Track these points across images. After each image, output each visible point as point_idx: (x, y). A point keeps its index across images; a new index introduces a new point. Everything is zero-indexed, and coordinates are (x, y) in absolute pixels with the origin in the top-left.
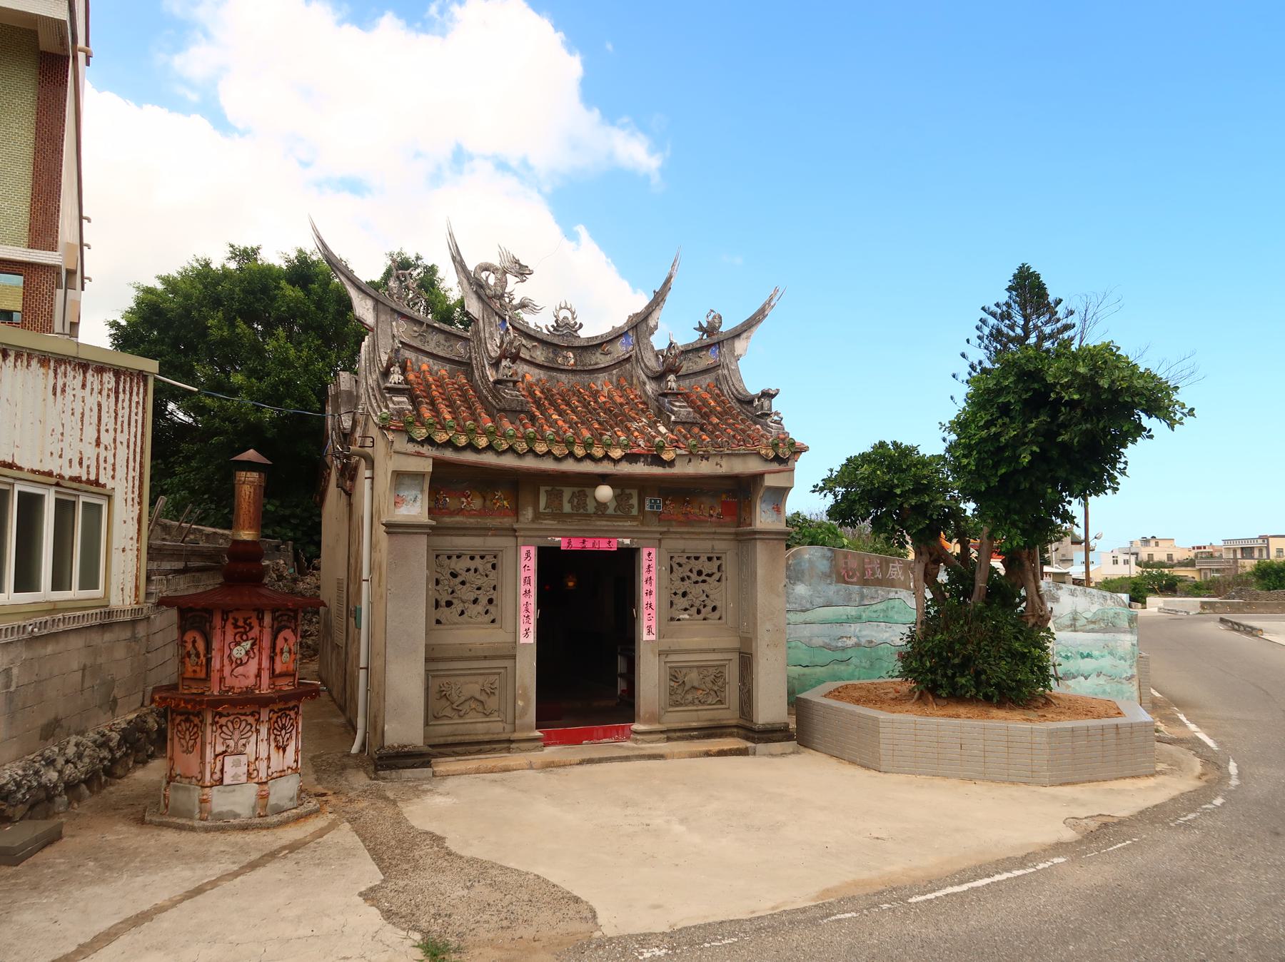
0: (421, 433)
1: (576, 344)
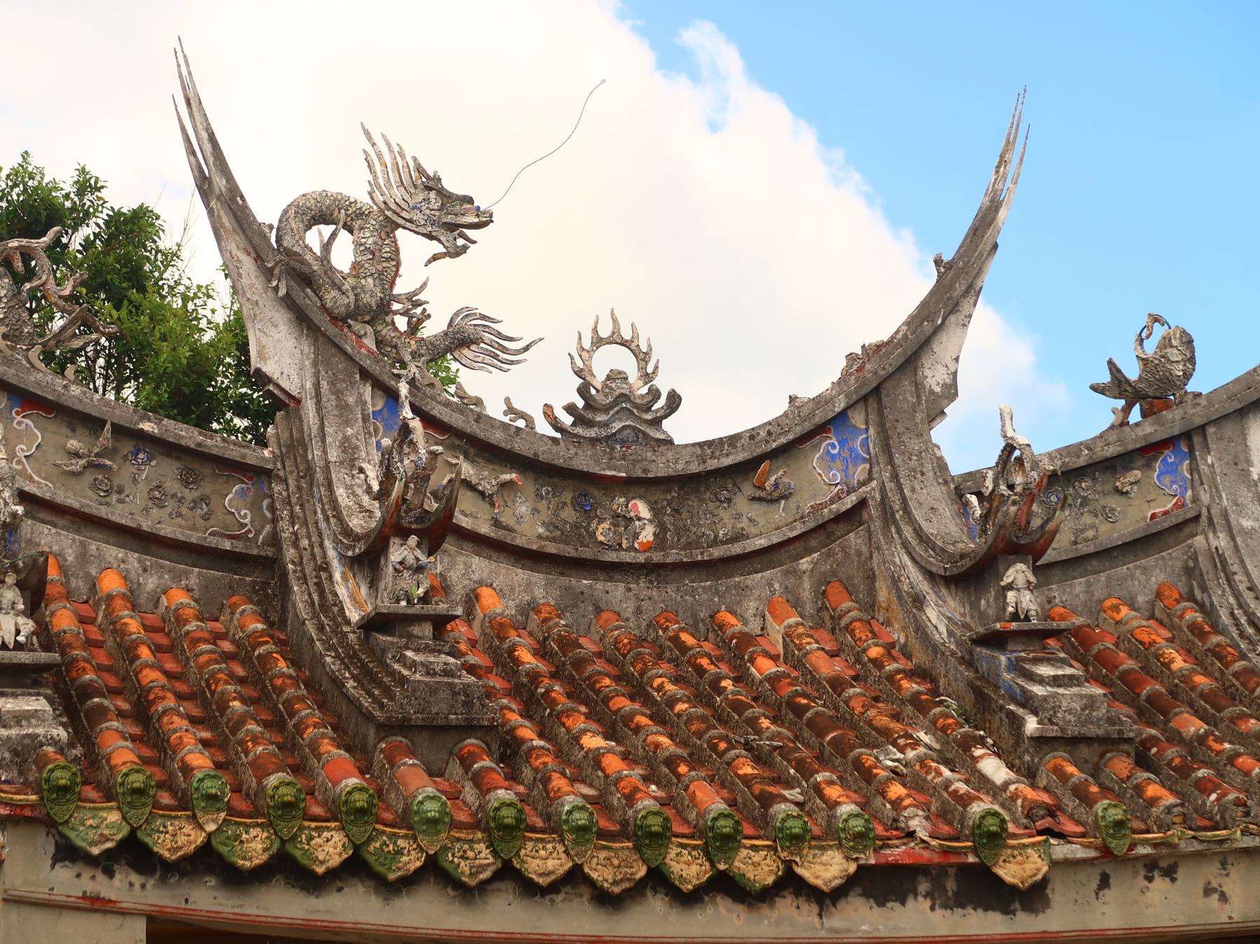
0: (102, 825)
1: (661, 468)
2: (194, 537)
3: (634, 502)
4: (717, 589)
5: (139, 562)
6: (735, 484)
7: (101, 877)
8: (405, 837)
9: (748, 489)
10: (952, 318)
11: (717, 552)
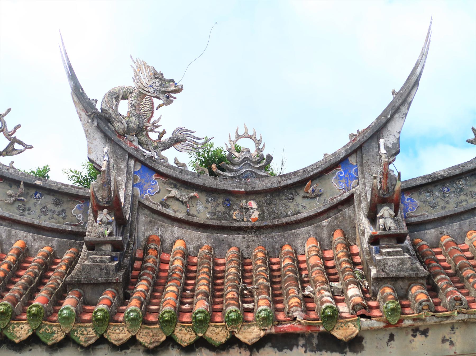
2: (56, 226)
3: (250, 201)
4: (284, 237)
5: (32, 236)
6: (296, 192)
8: (56, 326)
9: (302, 193)
10: (397, 115)
11: (284, 220)
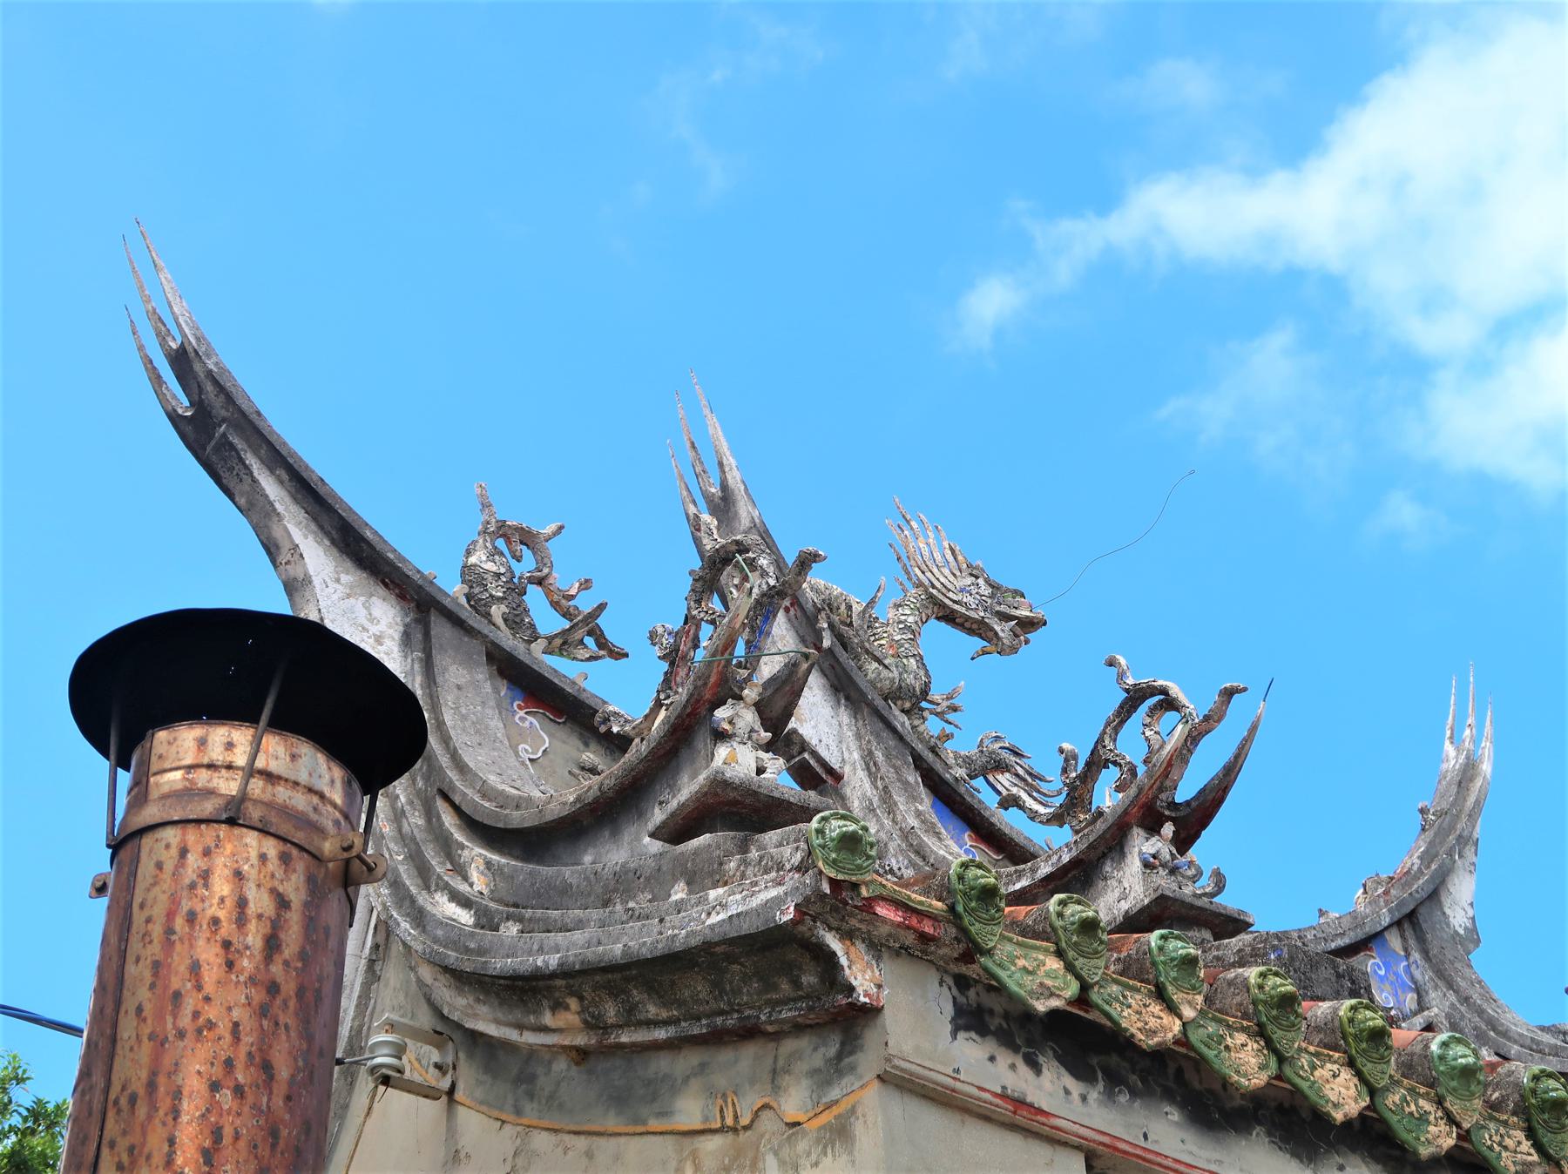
7: (1023, 1068)
